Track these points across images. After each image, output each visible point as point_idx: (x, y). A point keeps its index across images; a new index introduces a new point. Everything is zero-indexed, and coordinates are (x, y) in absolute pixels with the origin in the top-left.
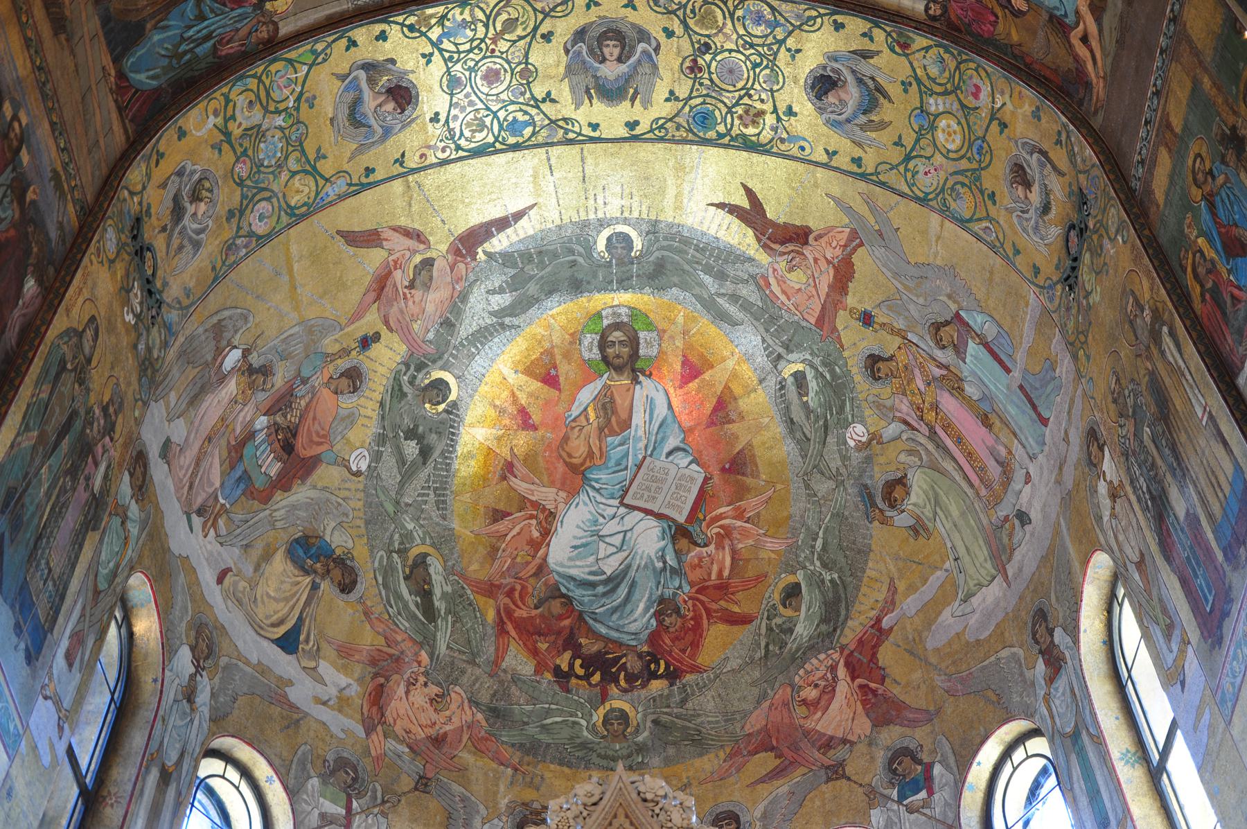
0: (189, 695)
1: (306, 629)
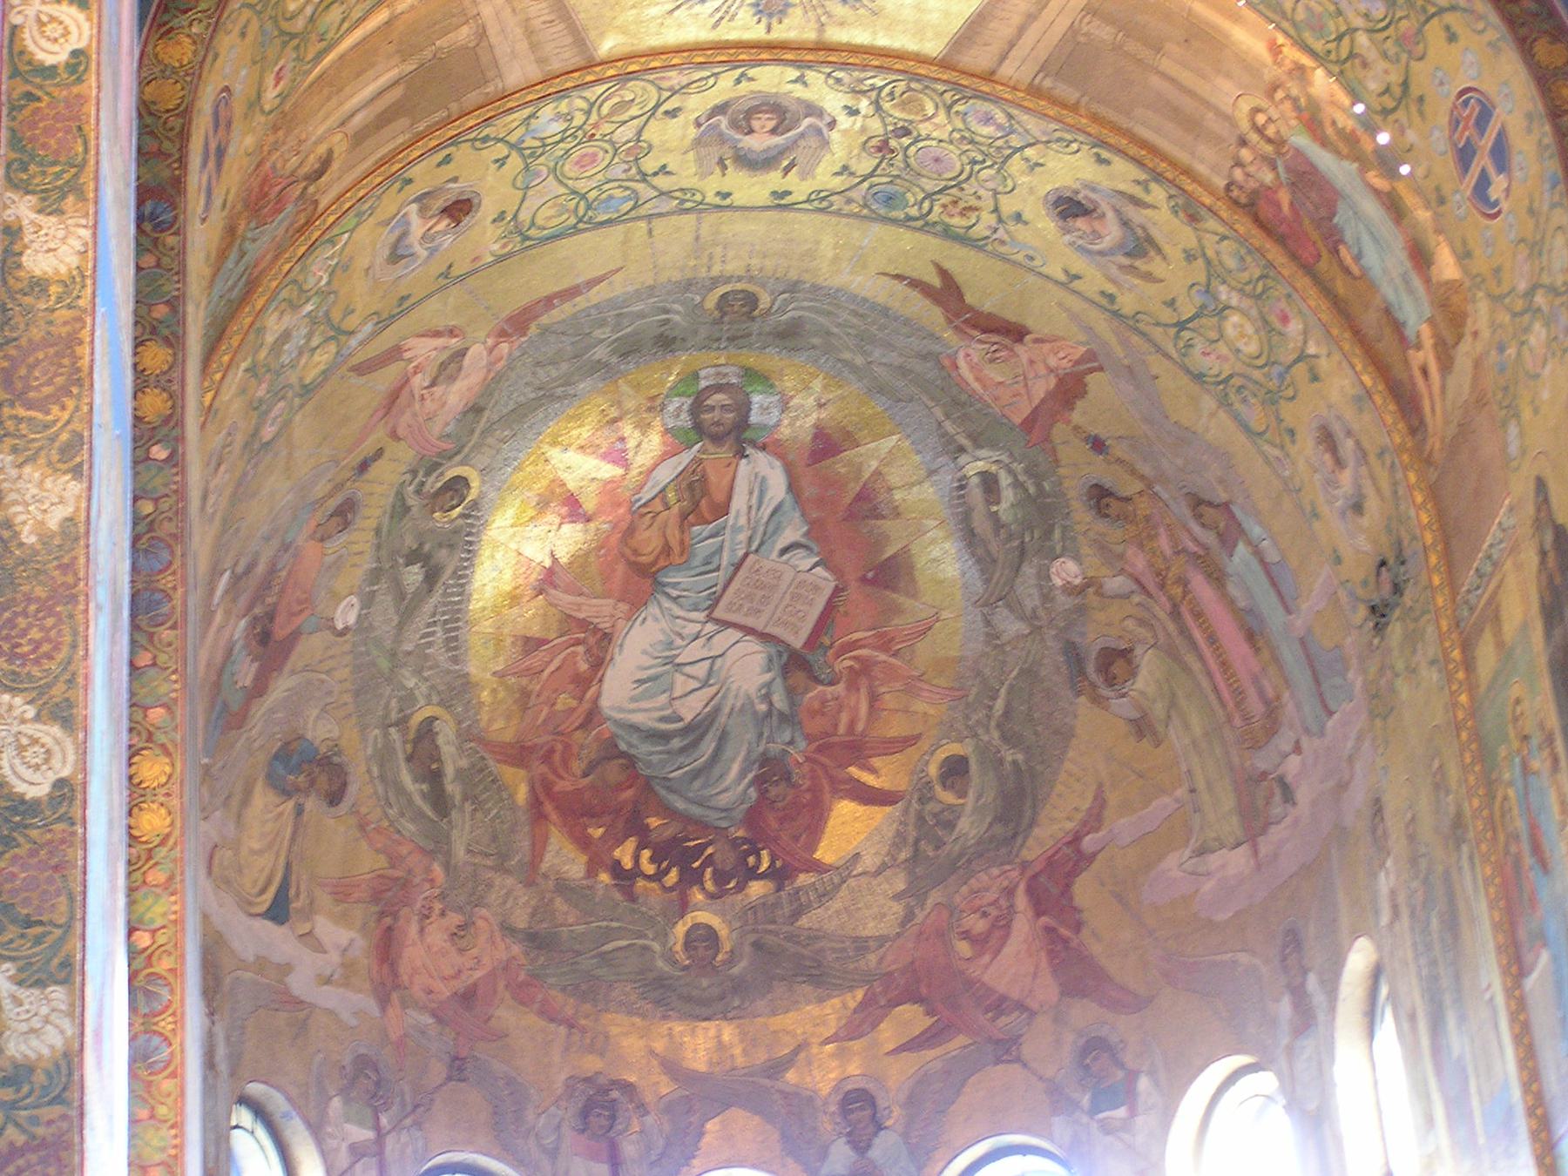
1: (294, 877)
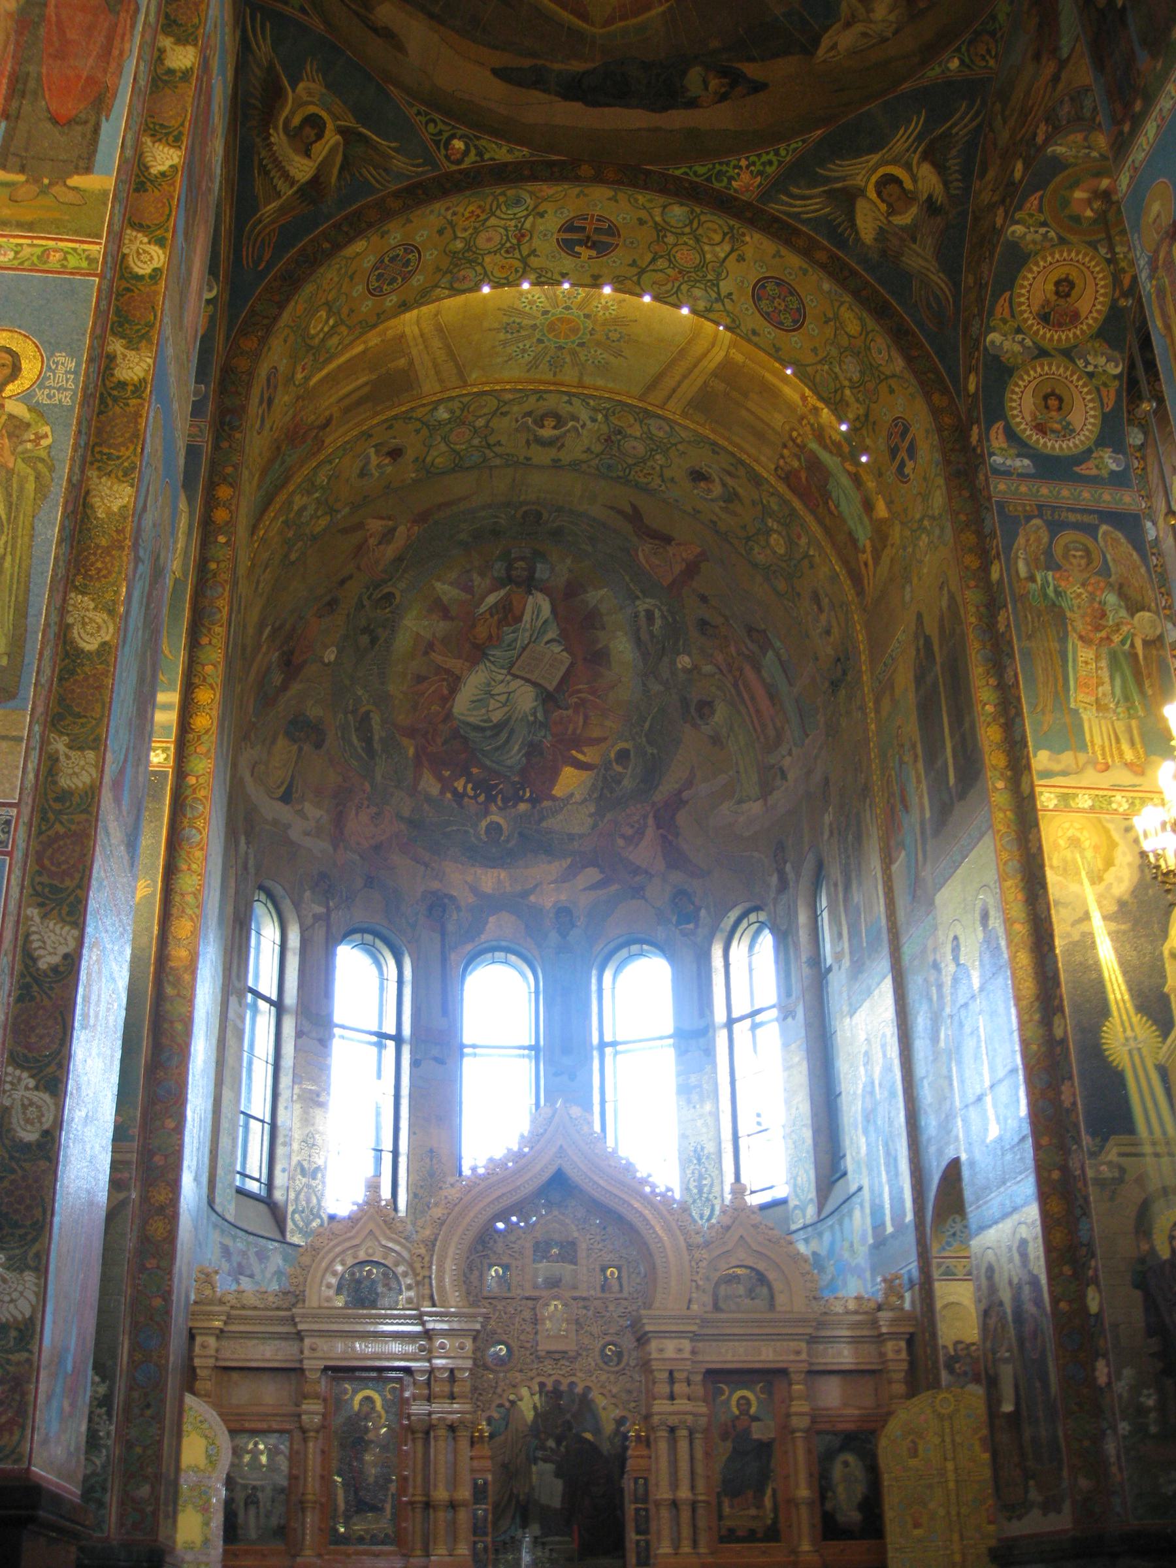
0: (245, 868)
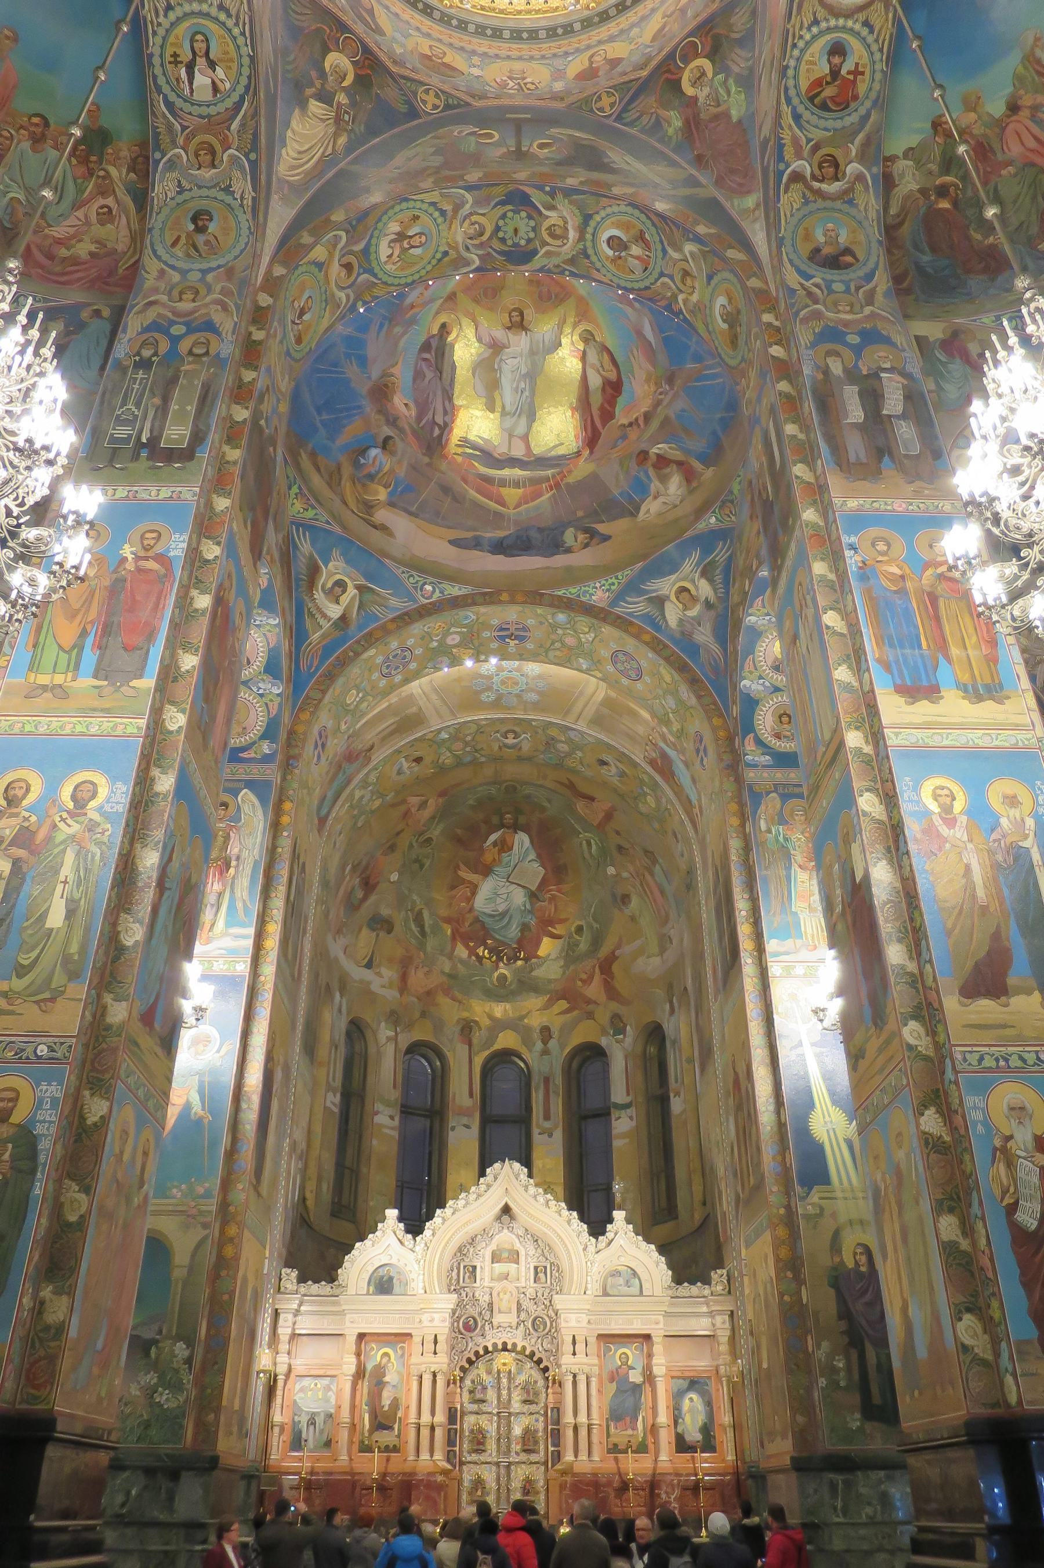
0: (340, 1011)
